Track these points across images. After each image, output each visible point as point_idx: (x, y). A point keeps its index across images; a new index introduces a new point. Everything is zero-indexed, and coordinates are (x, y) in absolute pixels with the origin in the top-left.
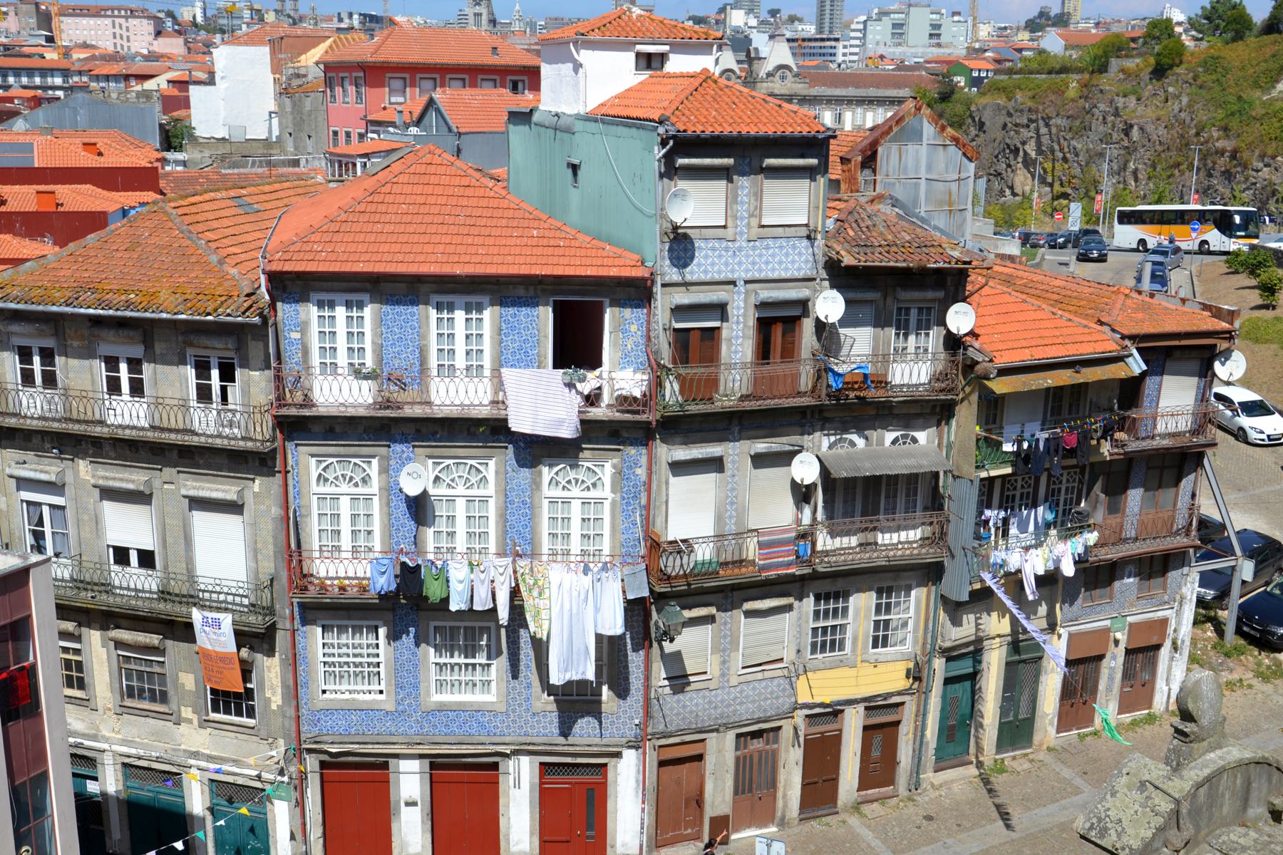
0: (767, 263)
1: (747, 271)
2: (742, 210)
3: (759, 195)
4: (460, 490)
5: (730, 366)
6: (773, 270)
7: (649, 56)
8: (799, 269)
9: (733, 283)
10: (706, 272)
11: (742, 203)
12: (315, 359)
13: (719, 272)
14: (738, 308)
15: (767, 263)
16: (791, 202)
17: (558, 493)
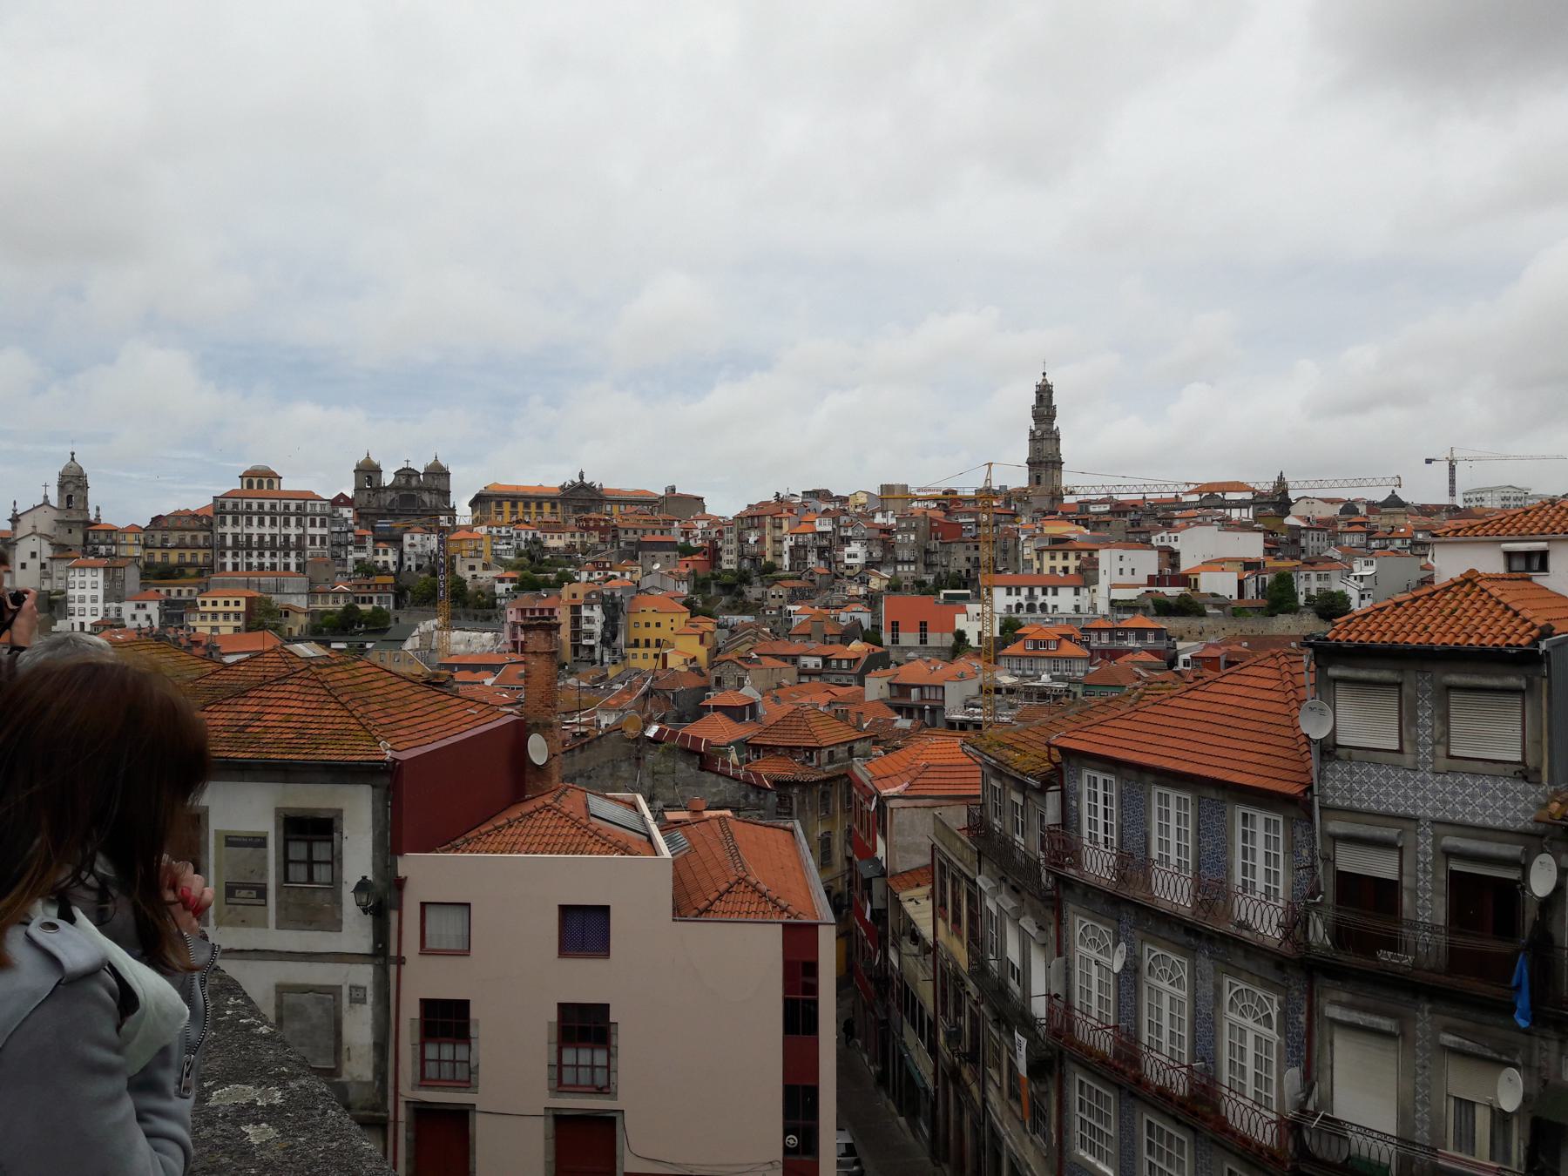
0: (1464, 804)
1: (1435, 810)
2: (1425, 735)
3: (1445, 719)
4: (1165, 985)
5: (1414, 925)
6: (1474, 814)
7: (1528, 555)
8: (1515, 819)
9: (1416, 819)
10: (1378, 802)
11: (1424, 726)
12: (1085, 831)
13: (1396, 805)
14: (1425, 853)
15: (1464, 804)
16: (1493, 733)
17: (1234, 1016)
